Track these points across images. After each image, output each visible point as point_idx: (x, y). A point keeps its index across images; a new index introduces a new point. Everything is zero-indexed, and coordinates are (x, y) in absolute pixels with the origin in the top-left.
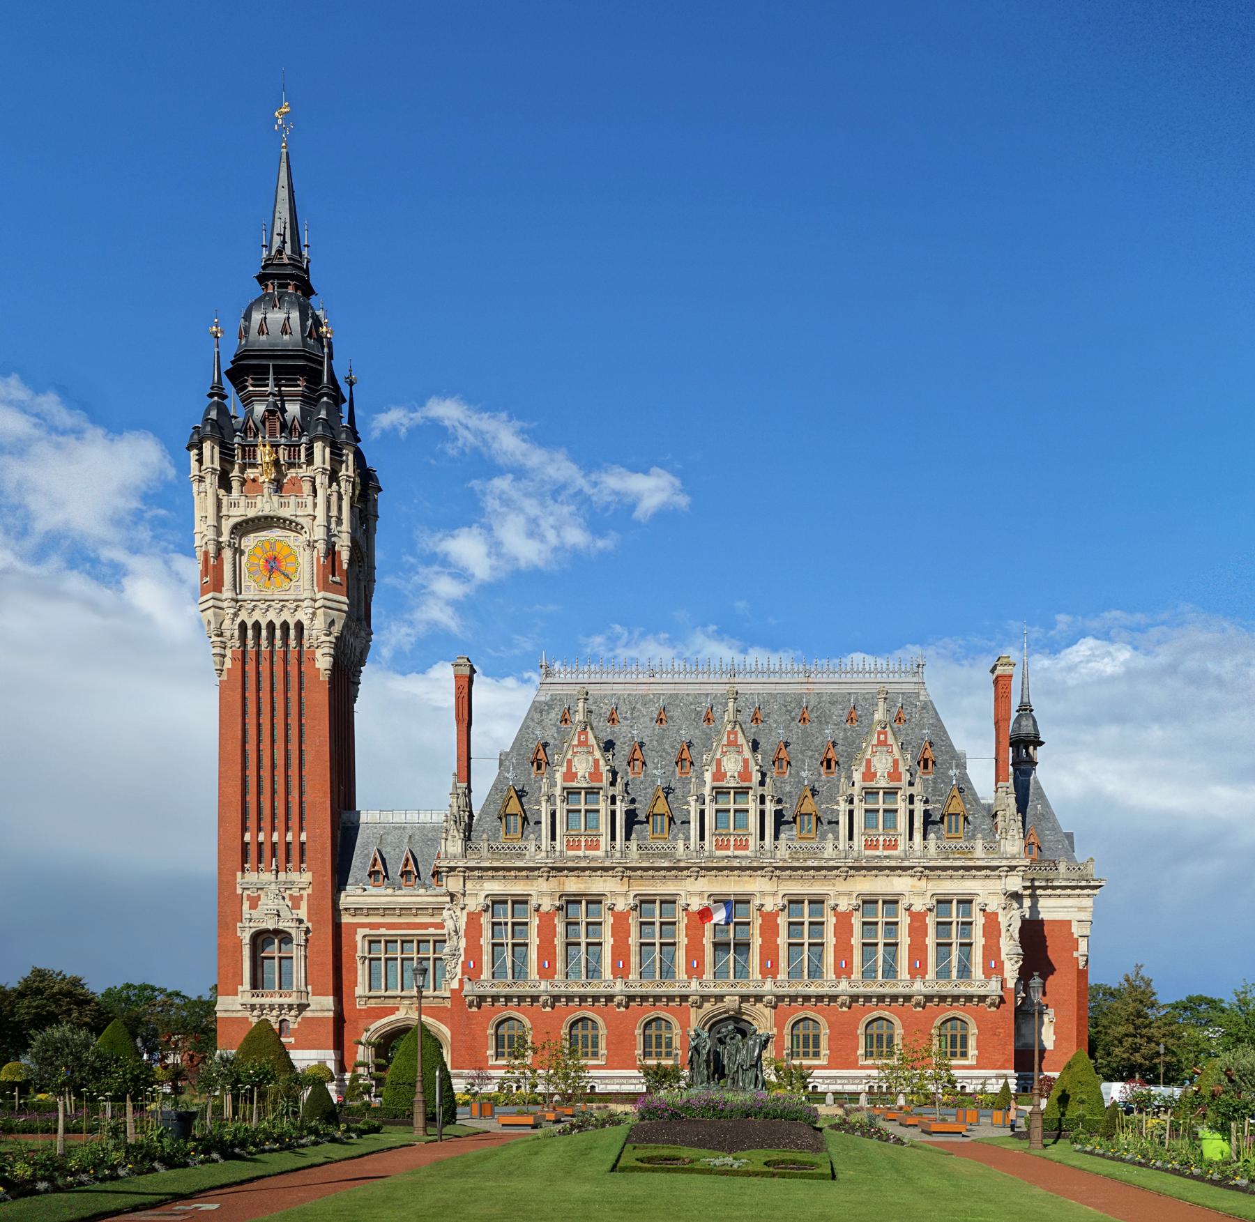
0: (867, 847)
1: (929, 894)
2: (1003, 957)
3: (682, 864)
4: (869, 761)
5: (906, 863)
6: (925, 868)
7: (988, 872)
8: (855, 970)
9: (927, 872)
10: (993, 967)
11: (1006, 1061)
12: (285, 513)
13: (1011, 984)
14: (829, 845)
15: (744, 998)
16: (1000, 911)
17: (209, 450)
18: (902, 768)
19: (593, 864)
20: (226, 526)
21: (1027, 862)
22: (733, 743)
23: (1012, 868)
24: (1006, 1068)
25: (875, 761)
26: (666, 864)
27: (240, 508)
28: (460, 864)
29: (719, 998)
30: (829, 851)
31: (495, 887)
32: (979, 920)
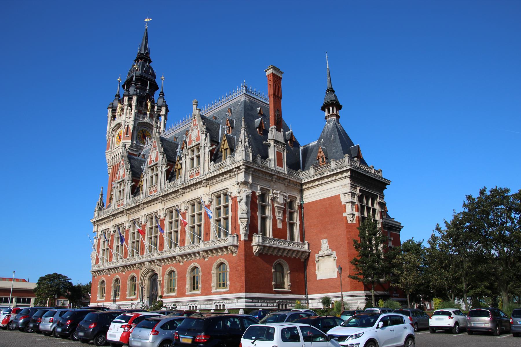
0: (191, 176)
1: (210, 193)
2: (239, 221)
3: (138, 204)
4: (190, 135)
5: (198, 180)
6: (207, 180)
7: (230, 174)
8: (186, 242)
9: (209, 182)
10: (236, 228)
11: (242, 287)
12: (120, 122)
13: (243, 238)
14: (179, 180)
15: (150, 262)
16: (238, 195)
17: (110, 110)
18: (200, 134)
19: (119, 211)
20: (111, 130)
21: (242, 163)
22: (155, 147)
23: (238, 168)
24: (241, 292)
25: (192, 136)
26: (134, 205)
27: (114, 123)
28: (95, 220)
29: (143, 263)
30: (179, 183)
31: (103, 227)
32: (230, 202)
